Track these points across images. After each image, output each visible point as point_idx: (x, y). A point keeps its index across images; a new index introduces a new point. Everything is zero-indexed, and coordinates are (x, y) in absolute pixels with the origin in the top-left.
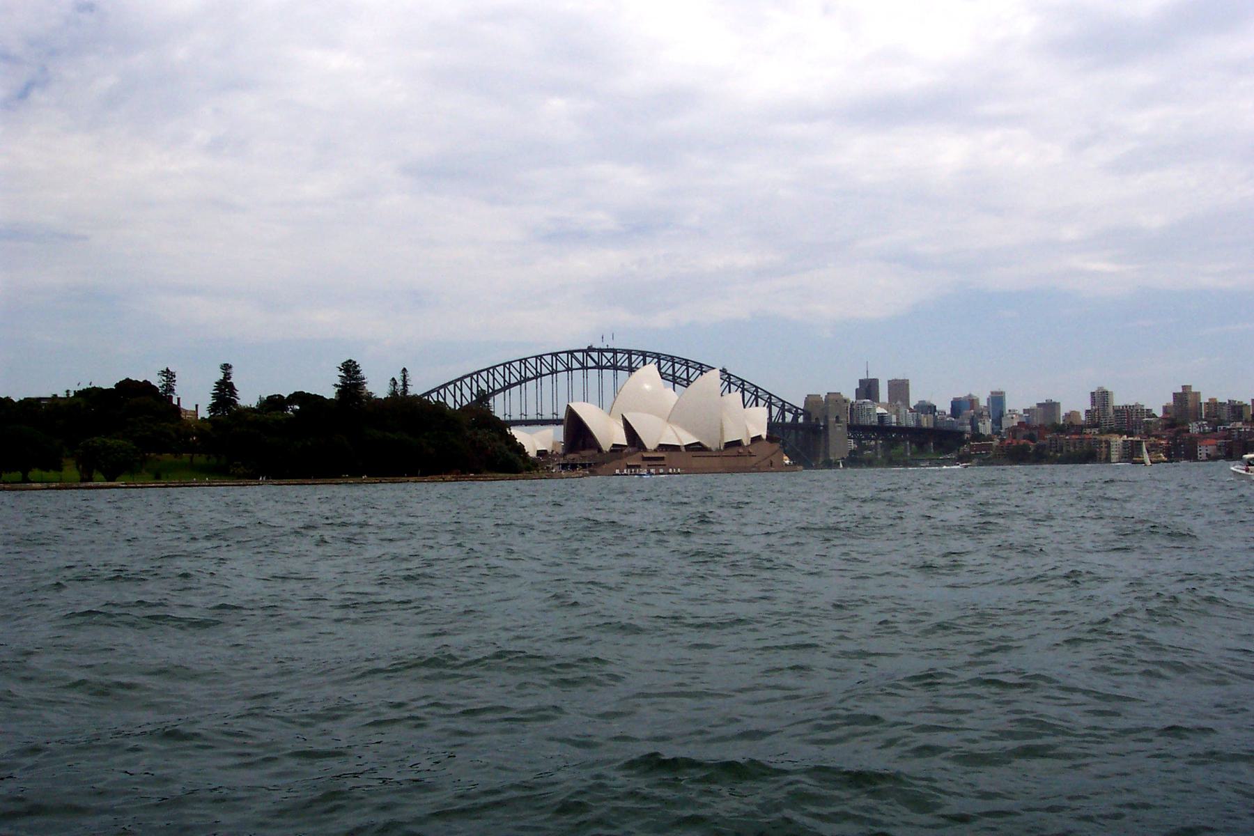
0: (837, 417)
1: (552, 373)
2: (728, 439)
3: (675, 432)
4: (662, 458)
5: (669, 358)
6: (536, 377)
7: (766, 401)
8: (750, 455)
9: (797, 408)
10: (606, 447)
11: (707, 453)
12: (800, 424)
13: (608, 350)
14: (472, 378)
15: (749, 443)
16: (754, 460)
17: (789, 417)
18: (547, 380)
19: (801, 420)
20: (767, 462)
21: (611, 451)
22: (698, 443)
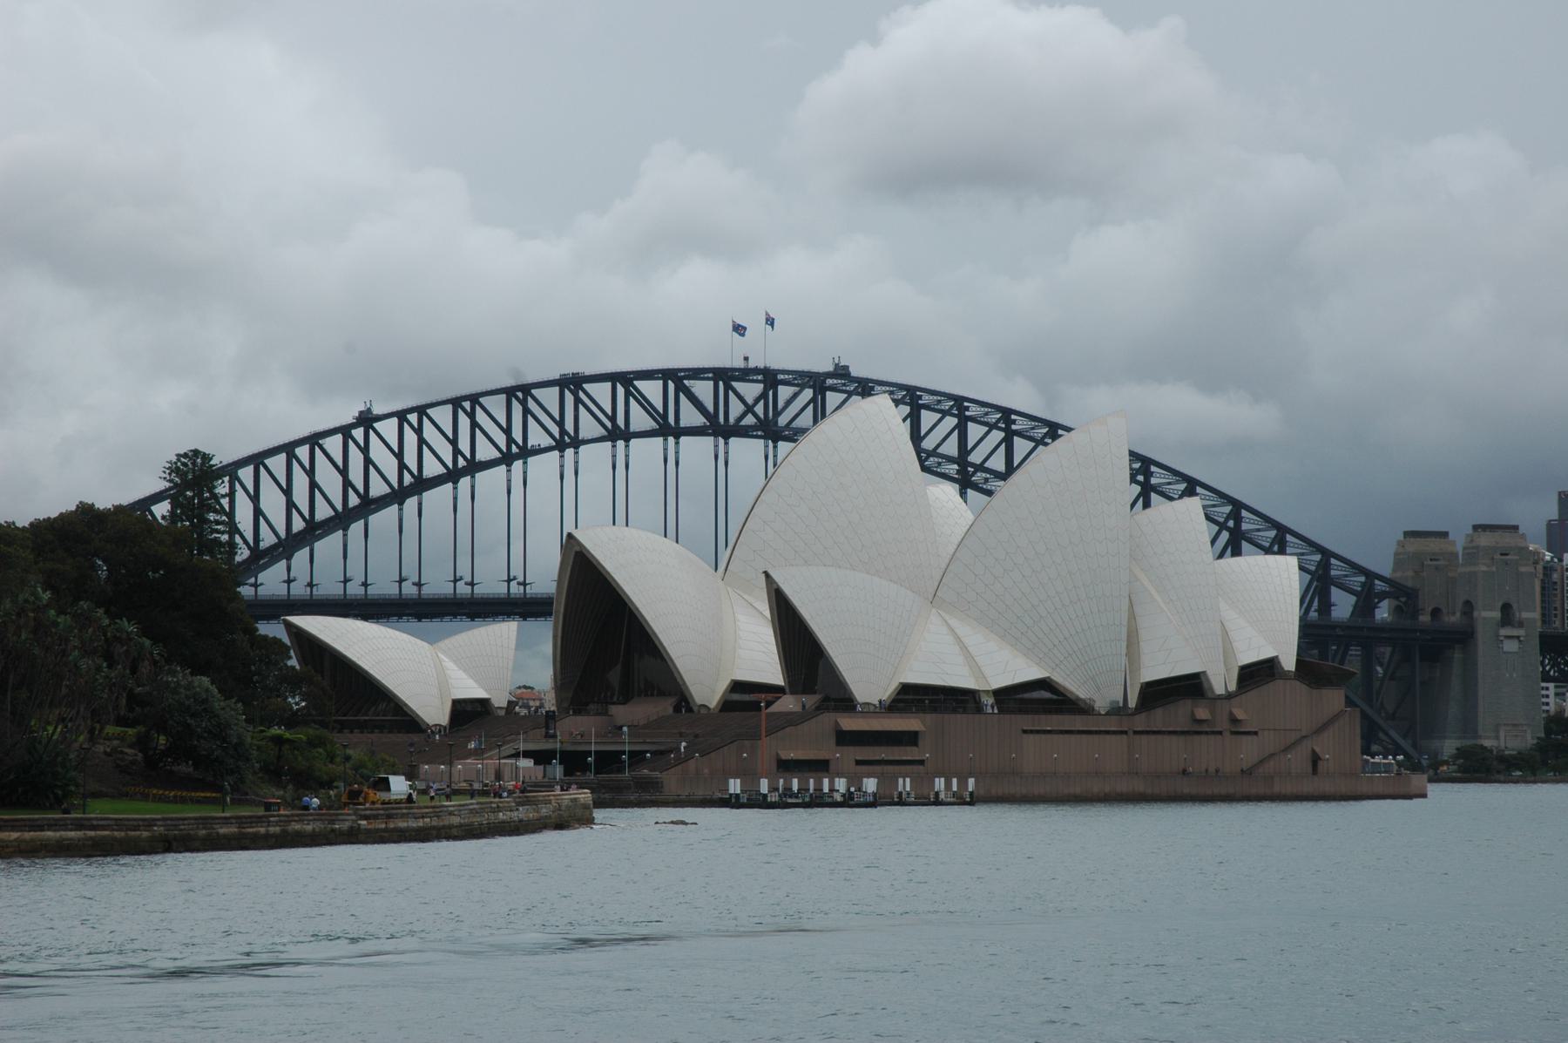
0: (1506, 608)
1: (560, 446)
2: (1157, 668)
3: (958, 639)
4: (911, 738)
5: (948, 405)
6: (507, 459)
8: (1237, 729)
9: (1370, 575)
10: (707, 690)
11: (1077, 722)
12: (1383, 628)
13: (745, 374)
14: (291, 456)
15: (1233, 687)
16: (1248, 752)
18: (543, 467)
19: (1383, 612)
20: (1297, 760)
21: (727, 706)
22: (1044, 684)
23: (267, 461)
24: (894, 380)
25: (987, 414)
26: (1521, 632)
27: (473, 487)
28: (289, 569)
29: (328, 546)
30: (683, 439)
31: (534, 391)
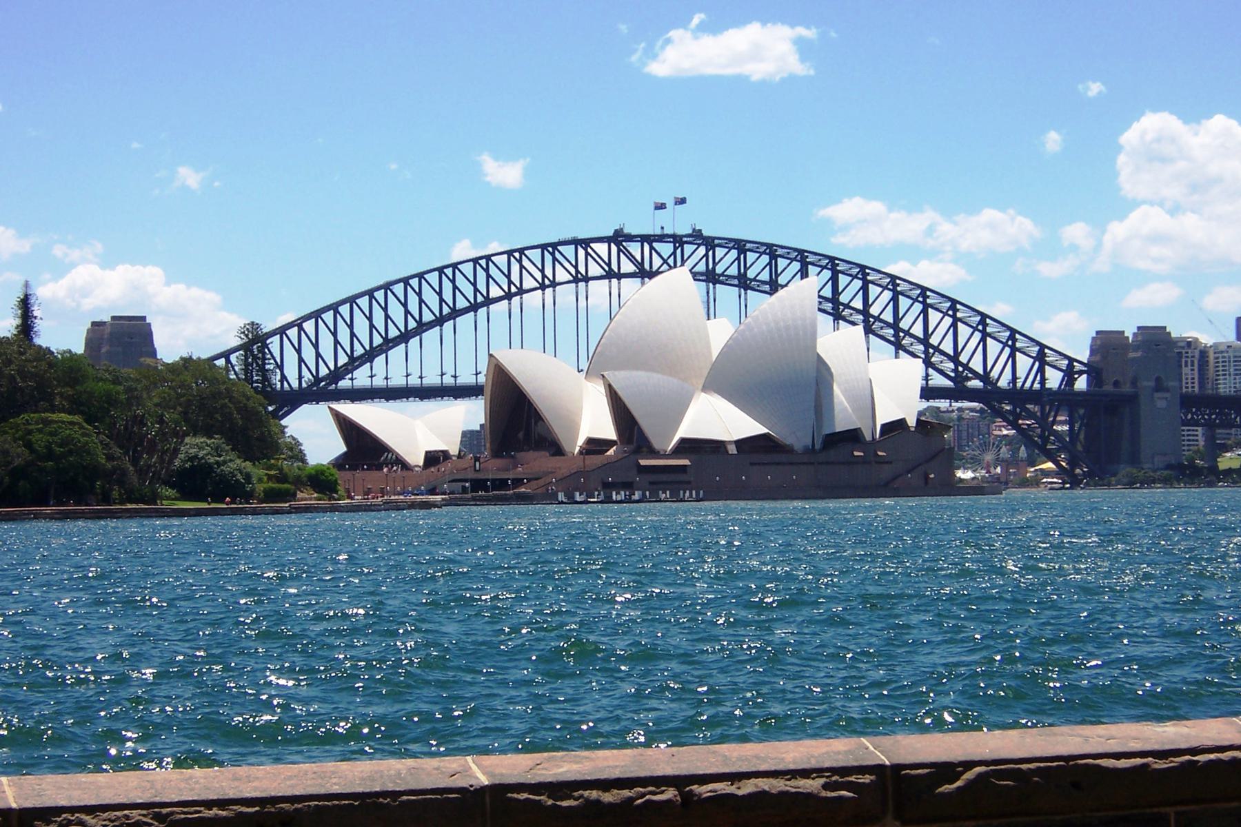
0: (1158, 380)
6: (509, 296)
7: (1005, 345)
9: (1071, 360)
11: (783, 458)
12: (1080, 393)
13: (661, 238)
14: (372, 297)
16: (886, 472)
17: (1054, 379)
19: (1081, 383)
23: (357, 301)
24: (758, 240)
25: (820, 260)
26: (1167, 395)
27: (488, 314)
28: (371, 369)
29: (397, 353)
30: (623, 280)
31: (526, 252)
